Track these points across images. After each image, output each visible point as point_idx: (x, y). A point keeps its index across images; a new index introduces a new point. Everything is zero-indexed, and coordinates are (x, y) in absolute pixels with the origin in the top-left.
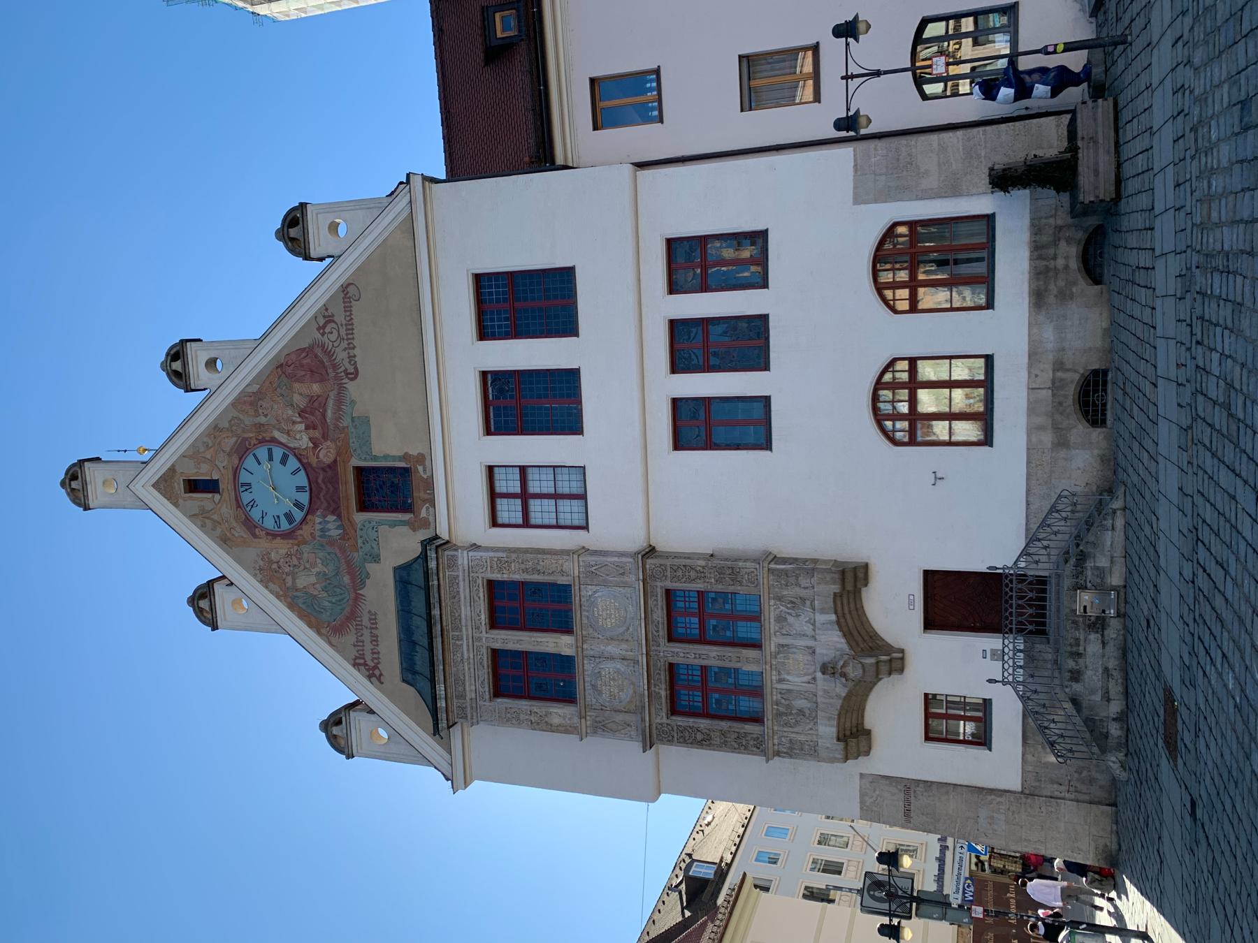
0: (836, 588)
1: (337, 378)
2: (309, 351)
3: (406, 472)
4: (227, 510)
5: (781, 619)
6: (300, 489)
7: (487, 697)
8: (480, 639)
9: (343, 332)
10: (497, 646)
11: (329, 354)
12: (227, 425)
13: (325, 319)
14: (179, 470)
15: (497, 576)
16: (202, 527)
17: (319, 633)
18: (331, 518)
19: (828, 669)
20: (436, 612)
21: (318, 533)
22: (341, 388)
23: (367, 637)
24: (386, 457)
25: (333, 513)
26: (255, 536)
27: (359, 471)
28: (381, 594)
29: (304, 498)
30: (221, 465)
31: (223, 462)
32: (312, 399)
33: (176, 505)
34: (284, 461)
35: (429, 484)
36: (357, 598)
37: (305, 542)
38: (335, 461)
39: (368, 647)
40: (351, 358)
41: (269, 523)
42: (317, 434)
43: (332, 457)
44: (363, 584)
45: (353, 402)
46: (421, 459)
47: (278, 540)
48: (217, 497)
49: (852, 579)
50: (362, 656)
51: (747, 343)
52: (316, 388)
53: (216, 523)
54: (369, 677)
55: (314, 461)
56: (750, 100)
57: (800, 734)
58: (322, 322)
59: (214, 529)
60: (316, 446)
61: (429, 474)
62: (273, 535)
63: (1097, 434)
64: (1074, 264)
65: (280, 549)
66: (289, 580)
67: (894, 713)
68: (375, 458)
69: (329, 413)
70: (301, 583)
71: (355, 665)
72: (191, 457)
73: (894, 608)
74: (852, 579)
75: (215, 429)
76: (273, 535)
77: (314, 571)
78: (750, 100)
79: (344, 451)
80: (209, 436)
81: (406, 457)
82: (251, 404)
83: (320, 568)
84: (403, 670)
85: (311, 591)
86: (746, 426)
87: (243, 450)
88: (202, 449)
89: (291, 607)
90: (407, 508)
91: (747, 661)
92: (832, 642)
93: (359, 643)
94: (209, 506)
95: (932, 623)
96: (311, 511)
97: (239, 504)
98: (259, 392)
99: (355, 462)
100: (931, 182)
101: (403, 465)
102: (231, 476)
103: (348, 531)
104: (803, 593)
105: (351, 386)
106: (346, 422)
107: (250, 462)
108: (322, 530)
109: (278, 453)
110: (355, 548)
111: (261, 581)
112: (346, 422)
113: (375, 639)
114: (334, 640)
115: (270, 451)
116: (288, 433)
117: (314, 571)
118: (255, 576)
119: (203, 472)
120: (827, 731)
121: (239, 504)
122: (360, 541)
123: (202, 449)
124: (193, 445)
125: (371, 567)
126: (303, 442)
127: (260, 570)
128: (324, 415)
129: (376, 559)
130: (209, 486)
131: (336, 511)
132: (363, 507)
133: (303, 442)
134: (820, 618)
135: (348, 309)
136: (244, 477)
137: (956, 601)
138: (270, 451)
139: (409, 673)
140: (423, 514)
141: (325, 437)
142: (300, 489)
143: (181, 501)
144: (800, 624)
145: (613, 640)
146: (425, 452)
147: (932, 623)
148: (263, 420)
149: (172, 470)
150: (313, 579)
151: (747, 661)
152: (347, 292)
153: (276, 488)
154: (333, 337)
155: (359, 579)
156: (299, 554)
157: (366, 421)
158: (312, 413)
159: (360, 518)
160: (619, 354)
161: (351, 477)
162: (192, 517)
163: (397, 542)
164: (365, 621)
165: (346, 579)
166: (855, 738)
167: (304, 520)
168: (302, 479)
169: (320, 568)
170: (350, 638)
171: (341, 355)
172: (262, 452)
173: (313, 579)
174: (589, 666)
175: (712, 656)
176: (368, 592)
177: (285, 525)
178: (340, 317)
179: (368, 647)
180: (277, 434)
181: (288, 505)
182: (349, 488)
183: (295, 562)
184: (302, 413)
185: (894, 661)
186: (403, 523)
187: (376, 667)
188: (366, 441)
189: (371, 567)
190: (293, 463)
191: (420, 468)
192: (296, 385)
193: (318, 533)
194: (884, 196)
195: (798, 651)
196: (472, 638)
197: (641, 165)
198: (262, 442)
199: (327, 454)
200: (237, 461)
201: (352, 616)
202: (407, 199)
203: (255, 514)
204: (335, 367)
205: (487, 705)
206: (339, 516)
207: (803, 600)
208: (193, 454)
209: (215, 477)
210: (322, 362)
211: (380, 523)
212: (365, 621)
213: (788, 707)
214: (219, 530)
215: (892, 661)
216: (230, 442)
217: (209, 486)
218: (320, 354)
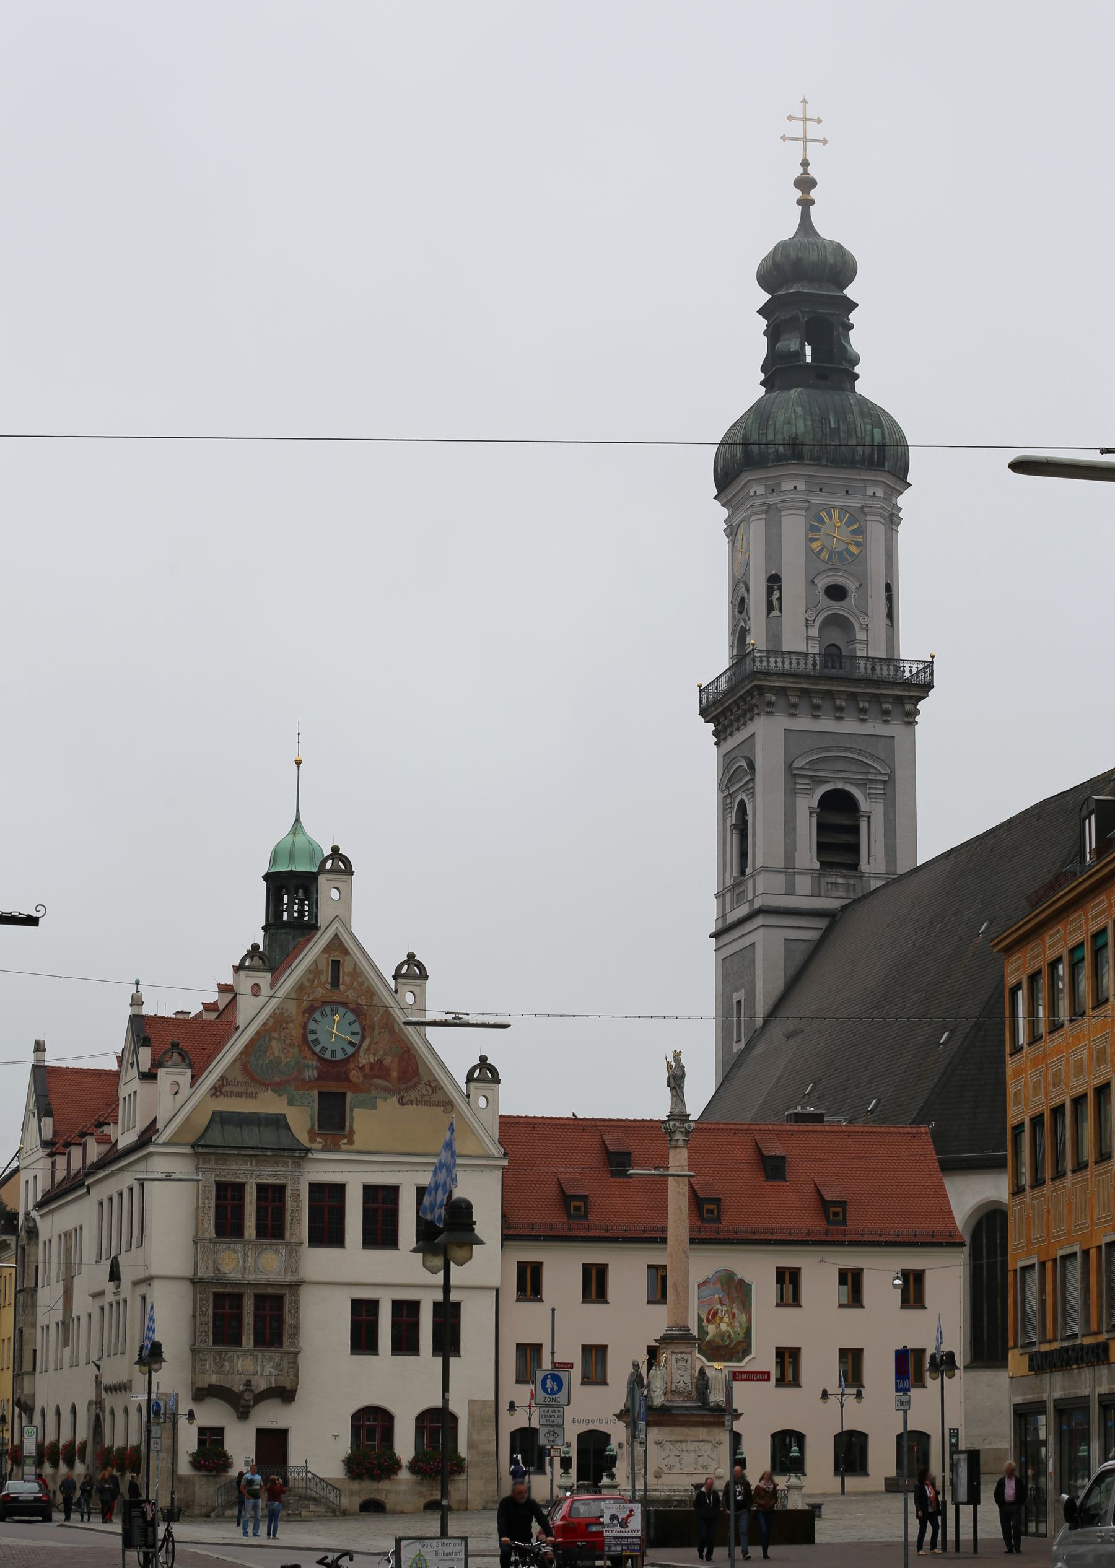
0: (288, 1387)
1: (400, 1090)
2: (416, 1073)
3: (343, 1128)
4: (320, 993)
5: (271, 1358)
6: (334, 1052)
7: (217, 1179)
8: (251, 1177)
9: (426, 1098)
10: (248, 1188)
11: (414, 1086)
12: (374, 1003)
13: (435, 1087)
14: (347, 958)
15: (288, 1192)
16: (309, 971)
17: (242, 1053)
18: (316, 1073)
19: (248, 1383)
20: (269, 1153)
21: (306, 1062)
22: (393, 1092)
23: (240, 1089)
24: (352, 1118)
25: (319, 1075)
26: (304, 1013)
27: (344, 1095)
28: (267, 1104)
29: (328, 1056)
30: (349, 993)
31: (351, 995)
32: (388, 1070)
33: (324, 951)
34: (351, 1043)
35: (336, 1149)
36: (265, 1085)
37: (300, 1051)
38: (350, 1081)
39: (235, 1089)
40: (410, 1102)
41: (312, 1026)
42: (367, 1070)
43: (353, 1079)
44: (274, 1091)
45: (385, 1100)
46: (351, 1142)
47: (302, 1031)
48: (329, 986)
49: (285, 1394)
50: (228, 1084)
51: (406, 1343)
52: (395, 1074)
53: (312, 981)
54: (214, 1088)
55: (351, 1065)
56: (521, 1347)
57: (209, 1365)
58: (433, 1084)
59: (308, 980)
60: (362, 1069)
61: (344, 1147)
62: (305, 1026)
63: (357, 1508)
64: (433, 1498)
65: (295, 1031)
66: (275, 1035)
67: (212, 1414)
68: (352, 1111)
69: (379, 1081)
70: (274, 1043)
71: (222, 1078)
72: (355, 969)
73: (270, 1416)
74: (285, 1394)
75: (371, 993)
76: (305, 1026)
77: (282, 1056)
78: (521, 1347)
79: (356, 1089)
80: (368, 987)
81: (352, 1132)
82: (387, 1024)
83: (285, 1060)
84: (221, 1113)
85: (269, 1051)
86: (363, 1339)
87: (358, 1012)
88: (360, 980)
89: (258, 1034)
90: (320, 1127)
91: (248, 1339)
92: (261, 1385)
93: (236, 1083)
94: (323, 978)
95: (261, 1433)
96: (321, 1060)
97: (325, 1003)
98: (394, 1031)
99: (349, 1096)
100: (475, 1436)
101: (347, 1129)
102: (344, 1000)
103: (304, 1084)
104: (285, 1371)
105: (395, 1099)
106: (374, 1093)
107: (351, 1017)
108: (308, 1066)
109: (356, 1040)
110: (297, 1088)
111: (274, 1013)
112: (374, 1093)
113: (239, 1095)
114: (238, 1063)
115: (357, 1034)
116: (368, 1049)
117: (282, 1056)
118: (278, 1008)
119: (344, 979)
120: (213, 1379)
121: (325, 1003)
122: (301, 1092)
123: (360, 980)
124: (362, 973)
125: (285, 1098)
126: (363, 1060)
127: (282, 1013)
128: (378, 1077)
129: (291, 1103)
130: (335, 982)
131: (320, 1077)
132: (320, 1093)
133: (363, 1060)
134: (273, 1379)
135: (439, 1104)
136: (342, 1010)
137: (273, 1444)
138: (357, 1034)
139: (221, 1119)
140: (318, 1140)
141: (365, 1076)
142: (334, 1052)
143: (326, 955)
144: (269, 1369)
145: (253, 1264)
146: (355, 1147)
147: (260, 1431)
148: (377, 1031)
149: (346, 952)
150: (276, 1054)
151: (248, 1339)
152: (448, 1105)
153: (335, 1032)
154: (424, 1091)
155: (278, 1088)
156: (292, 1045)
157: (374, 1107)
158: (378, 1070)
159: (315, 1093)
160: (401, 1271)
161: (340, 1090)
162: (316, 963)
163: (301, 1120)
164: (250, 1090)
165: (277, 1079)
166: (201, 1394)
167: (314, 1053)
168: (340, 1056)
169: (285, 1060)
170: (240, 1078)
171: (413, 1095)
172: (356, 1027)
173: (276, 1054)
174: (239, 1247)
175: (248, 1319)
176: (269, 1094)
177: (311, 1037)
178: (436, 1098)
179: (235, 1089)
180: (367, 1041)
181: (324, 1042)
182: (333, 1087)
183: (288, 1042)
184: (380, 1061)
185: (243, 1414)
186: (313, 1125)
187: (222, 1094)
188: (362, 1105)
189: (285, 1098)
190: (350, 1050)
191: (345, 1141)
192: (396, 1060)
193: (306, 1062)
194: (471, 1415)
195: (250, 1366)
196: (252, 1176)
197: (497, 1290)
198: (363, 1028)
199: (355, 1076)
200: (351, 1006)
201: (254, 1080)
202: (496, 1155)
203: (317, 1015)
204: (406, 1089)
205: (212, 1179)
206: (316, 1080)
207: (281, 1370)
208: (357, 973)
209: (342, 987)
210: (409, 1081)
211: (312, 1109)
212: (250, 1090)
213: (224, 1360)
214: (307, 984)
215: (243, 1414)
216: (363, 1001)
217: (335, 982)
218: (414, 1080)
